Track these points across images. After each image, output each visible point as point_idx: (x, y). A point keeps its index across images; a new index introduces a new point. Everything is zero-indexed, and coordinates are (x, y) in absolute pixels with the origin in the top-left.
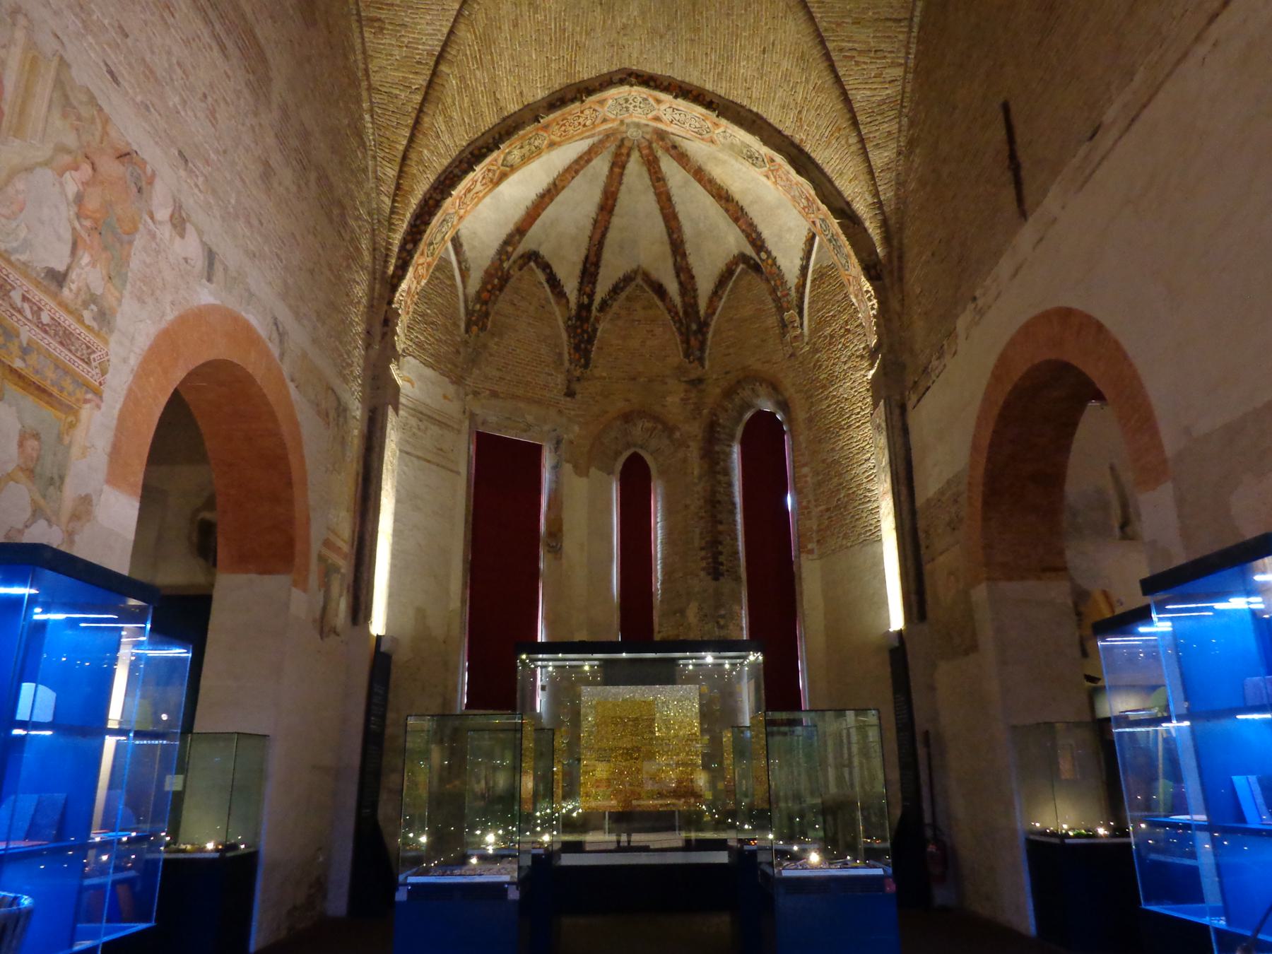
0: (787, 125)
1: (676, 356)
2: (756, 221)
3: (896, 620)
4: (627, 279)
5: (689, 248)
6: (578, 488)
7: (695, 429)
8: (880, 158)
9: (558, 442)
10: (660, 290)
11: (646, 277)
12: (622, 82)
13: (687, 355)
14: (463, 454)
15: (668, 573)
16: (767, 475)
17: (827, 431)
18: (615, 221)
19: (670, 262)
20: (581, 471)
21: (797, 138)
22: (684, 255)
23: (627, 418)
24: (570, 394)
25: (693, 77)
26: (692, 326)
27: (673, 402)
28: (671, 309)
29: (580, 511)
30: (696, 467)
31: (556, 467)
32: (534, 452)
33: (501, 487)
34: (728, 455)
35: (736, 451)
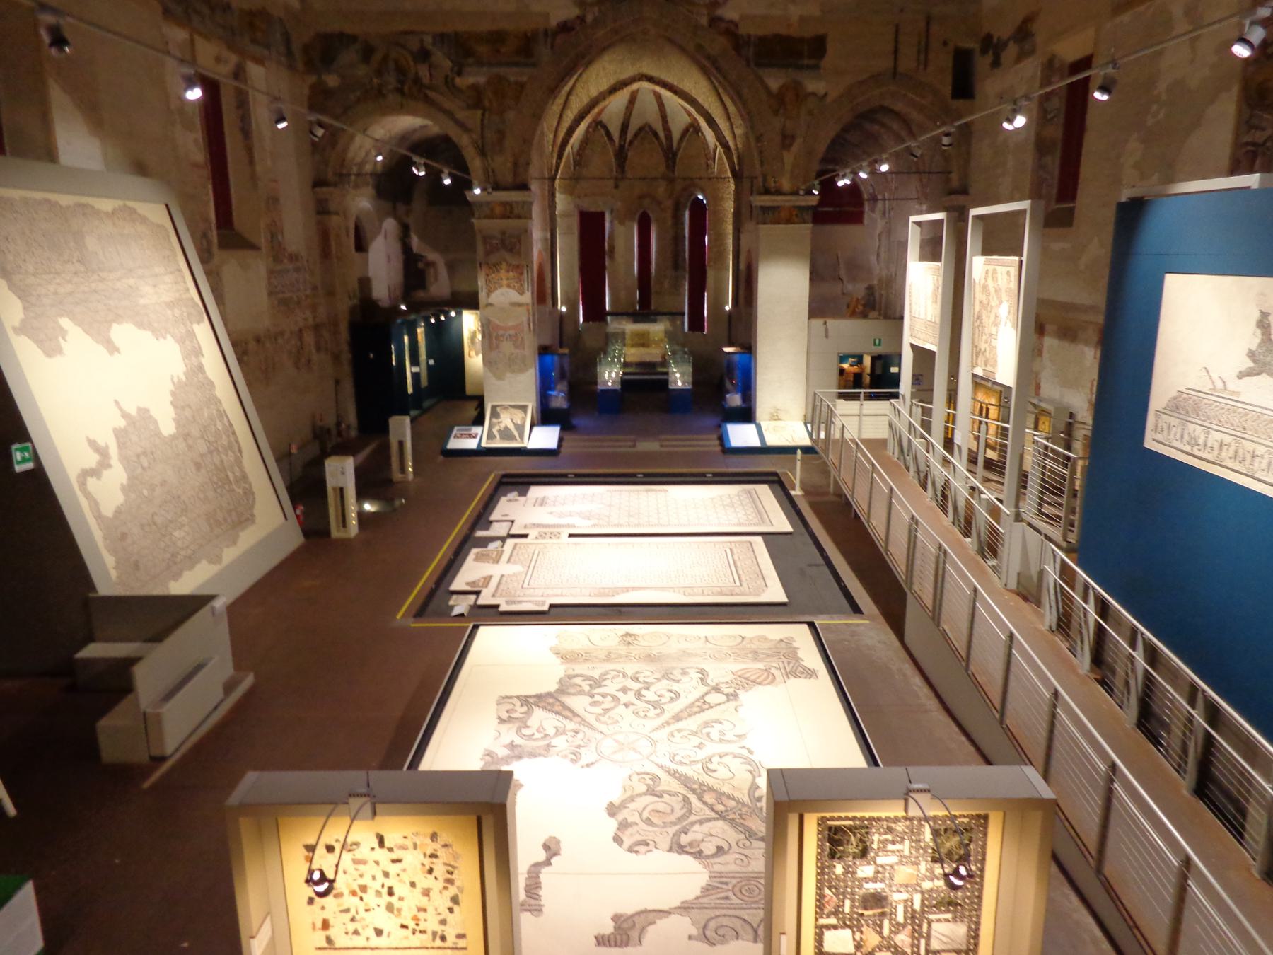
0: (706, 106)
1: (662, 168)
4: (641, 129)
6: (620, 230)
7: (669, 203)
8: (739, 132)
9: (612, 211)
10: (656, 134)
11: (650, 127)
12: (640, 80)
13: (668, 167)
14: (575, 222)
15: (657, 265)
16: (698, 229)
17: (719, 221)
18: (636, 105)
20: (622, 223)
23: (641, 197)
24: (616, 187)
25: (670, 79)
26: (670, 155)
27: (661, 189)
29: (623, 240)
30: (670, 222)
31: (611, 222)
32: (602, 215)
33: (591, 229)
34: (683, 215)
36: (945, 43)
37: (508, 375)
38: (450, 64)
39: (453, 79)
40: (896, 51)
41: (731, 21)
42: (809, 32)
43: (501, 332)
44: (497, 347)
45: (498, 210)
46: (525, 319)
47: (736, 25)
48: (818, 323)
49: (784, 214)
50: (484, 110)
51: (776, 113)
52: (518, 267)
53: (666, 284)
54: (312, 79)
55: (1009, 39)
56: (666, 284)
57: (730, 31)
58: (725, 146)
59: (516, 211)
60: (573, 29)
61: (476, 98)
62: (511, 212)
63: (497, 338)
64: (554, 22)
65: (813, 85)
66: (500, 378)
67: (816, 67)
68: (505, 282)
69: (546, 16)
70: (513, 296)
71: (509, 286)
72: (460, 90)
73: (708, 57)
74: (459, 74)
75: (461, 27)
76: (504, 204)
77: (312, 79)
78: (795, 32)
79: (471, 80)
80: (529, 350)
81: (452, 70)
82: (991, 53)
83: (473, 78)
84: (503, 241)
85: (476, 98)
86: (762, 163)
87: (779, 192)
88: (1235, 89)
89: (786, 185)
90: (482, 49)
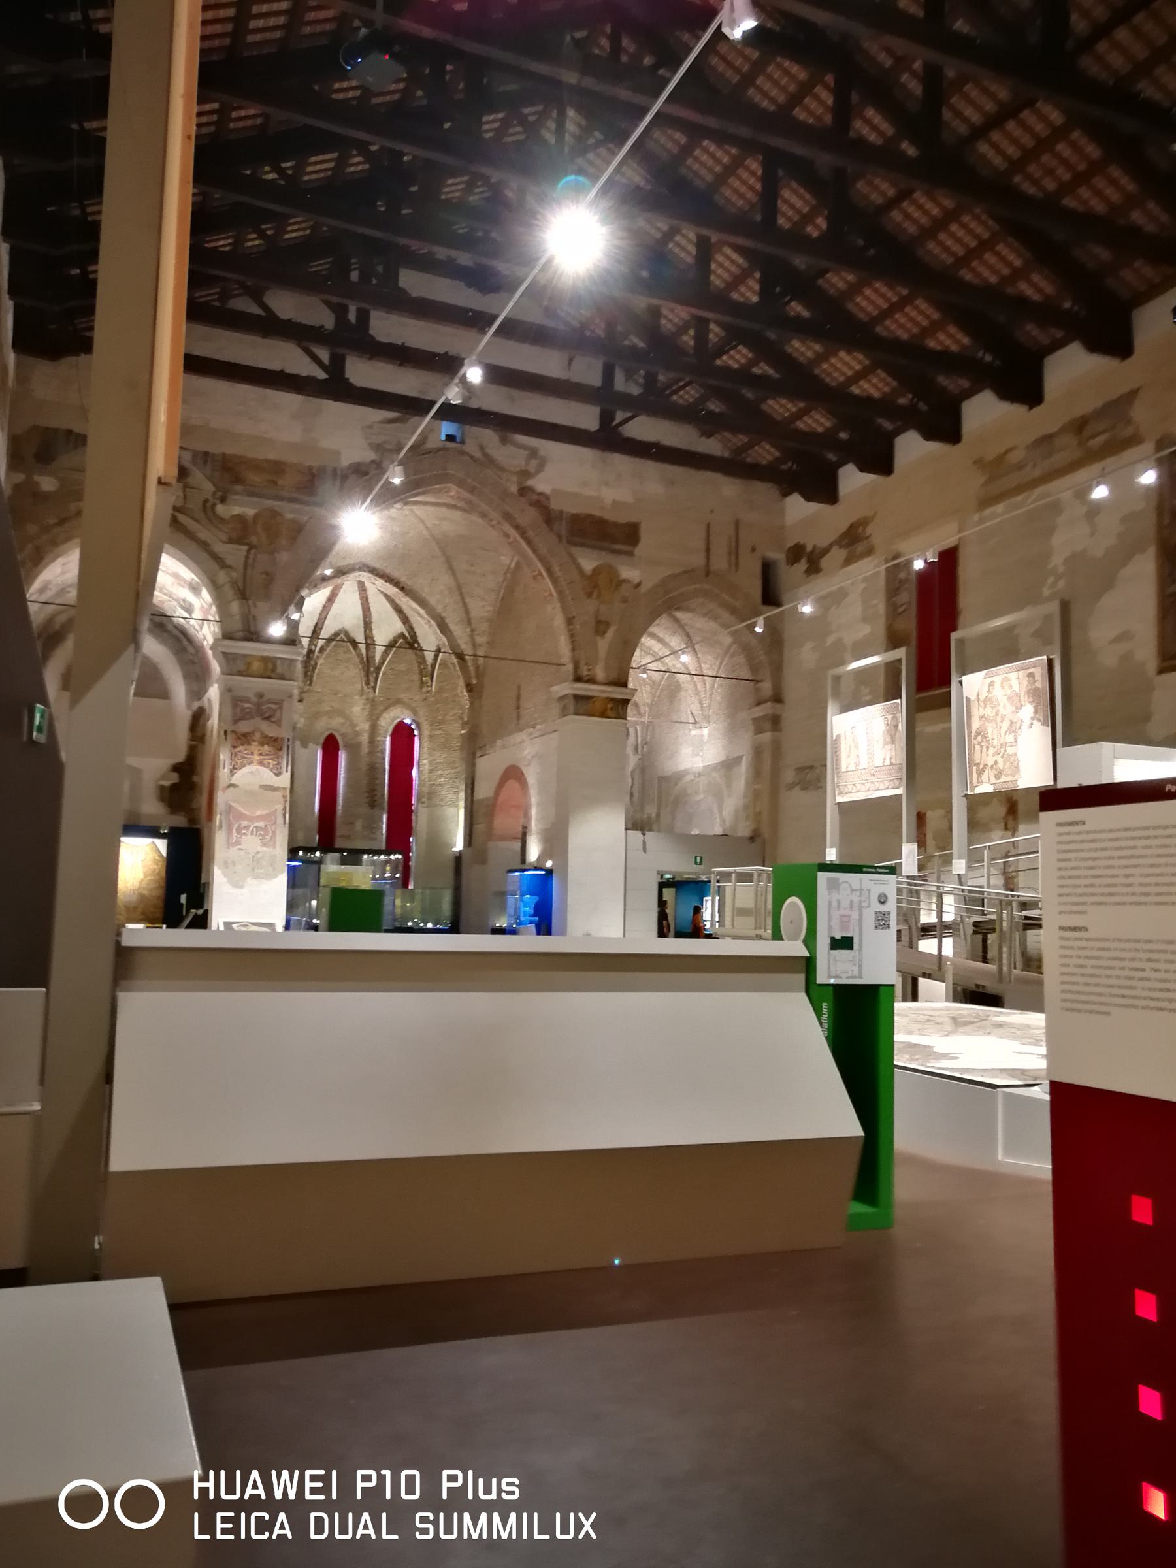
2: (414, 625)
3: (459, 845)
4: (336, 634)
5: (374, 626)
10: (354, 644)
11: (347, 634)
12: (360, 569)
13: (367, 683)
18: (335, 606)
19: (363, 630)
21: (443, 615)
22: (371, 630)
28: (360, 655)
35: (388, 740)
36: (753, 550)
37: (249, 880)
38: (212, 488)
39: (214, 505)
40: (708, 550)
41: (540, 494)
42: (623, 518)
43: (244, 823)
44: (238, 843)
45: (256, 666)
46: (280, 807)
47: (547, 498)
48: (636, 835)
49: (598, 706)
50: (252, 547)
51: (589, 595)
52: (276, 740)
53: (359, 825)
54: (20, 477)
55: (831, 545)
56: (359, 825)
57: (541, 503)
58: (460, 656)
59: (279, 670)
60: (366, 474)
61: (241, 532)
62: (273, 670)
63: (239, 830)
64: (345, 462)
65: (629, 573)
66: (237, 885)
67: (630, 554)
68: (257, 757)
69: (337, 454)
70: (266, 776)
71: (261, 764)
72: (222, 520)
73: (517, 527)
74: (223, 500)
75: (230, 450)
76: (265, 660)
77: (20, 477)
78: (610, 516)
79: (237, 510)
80: (280, 850)
81: (214, 493)
82: (804, 561)
83: (240, 507)
84: (258, 705)
85: (241, 532)
86: (573, 650)
87: (591, 681)
88: (1151, 552)
89: (600, 674)
90: (253, 477)
